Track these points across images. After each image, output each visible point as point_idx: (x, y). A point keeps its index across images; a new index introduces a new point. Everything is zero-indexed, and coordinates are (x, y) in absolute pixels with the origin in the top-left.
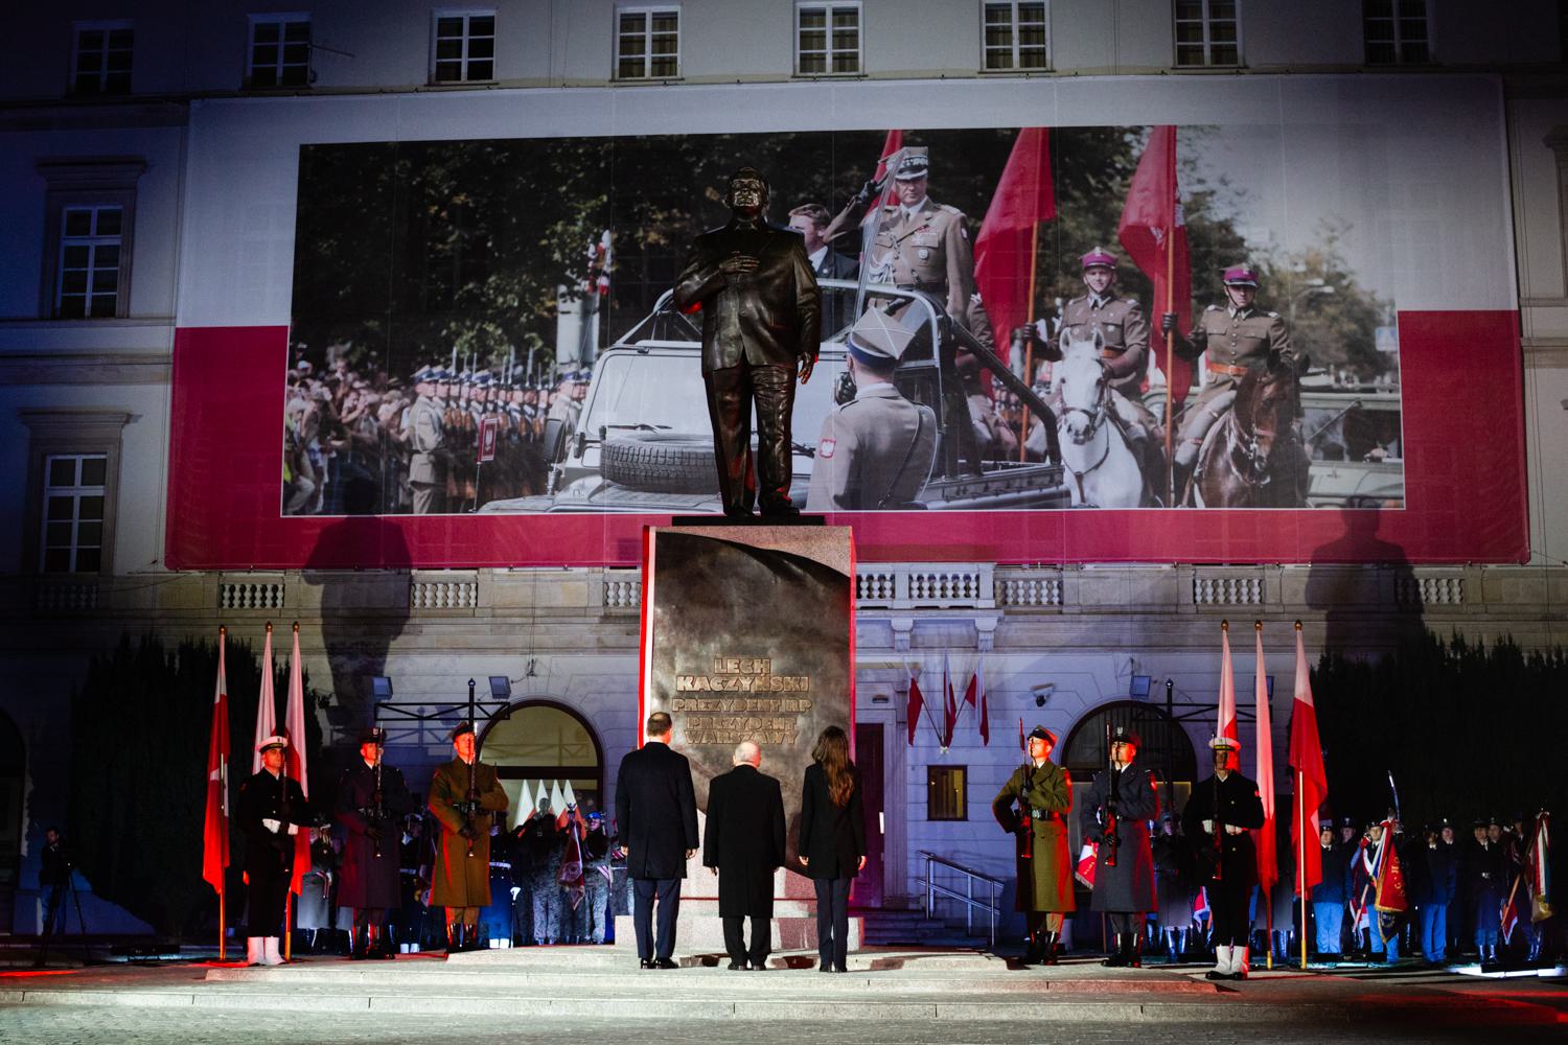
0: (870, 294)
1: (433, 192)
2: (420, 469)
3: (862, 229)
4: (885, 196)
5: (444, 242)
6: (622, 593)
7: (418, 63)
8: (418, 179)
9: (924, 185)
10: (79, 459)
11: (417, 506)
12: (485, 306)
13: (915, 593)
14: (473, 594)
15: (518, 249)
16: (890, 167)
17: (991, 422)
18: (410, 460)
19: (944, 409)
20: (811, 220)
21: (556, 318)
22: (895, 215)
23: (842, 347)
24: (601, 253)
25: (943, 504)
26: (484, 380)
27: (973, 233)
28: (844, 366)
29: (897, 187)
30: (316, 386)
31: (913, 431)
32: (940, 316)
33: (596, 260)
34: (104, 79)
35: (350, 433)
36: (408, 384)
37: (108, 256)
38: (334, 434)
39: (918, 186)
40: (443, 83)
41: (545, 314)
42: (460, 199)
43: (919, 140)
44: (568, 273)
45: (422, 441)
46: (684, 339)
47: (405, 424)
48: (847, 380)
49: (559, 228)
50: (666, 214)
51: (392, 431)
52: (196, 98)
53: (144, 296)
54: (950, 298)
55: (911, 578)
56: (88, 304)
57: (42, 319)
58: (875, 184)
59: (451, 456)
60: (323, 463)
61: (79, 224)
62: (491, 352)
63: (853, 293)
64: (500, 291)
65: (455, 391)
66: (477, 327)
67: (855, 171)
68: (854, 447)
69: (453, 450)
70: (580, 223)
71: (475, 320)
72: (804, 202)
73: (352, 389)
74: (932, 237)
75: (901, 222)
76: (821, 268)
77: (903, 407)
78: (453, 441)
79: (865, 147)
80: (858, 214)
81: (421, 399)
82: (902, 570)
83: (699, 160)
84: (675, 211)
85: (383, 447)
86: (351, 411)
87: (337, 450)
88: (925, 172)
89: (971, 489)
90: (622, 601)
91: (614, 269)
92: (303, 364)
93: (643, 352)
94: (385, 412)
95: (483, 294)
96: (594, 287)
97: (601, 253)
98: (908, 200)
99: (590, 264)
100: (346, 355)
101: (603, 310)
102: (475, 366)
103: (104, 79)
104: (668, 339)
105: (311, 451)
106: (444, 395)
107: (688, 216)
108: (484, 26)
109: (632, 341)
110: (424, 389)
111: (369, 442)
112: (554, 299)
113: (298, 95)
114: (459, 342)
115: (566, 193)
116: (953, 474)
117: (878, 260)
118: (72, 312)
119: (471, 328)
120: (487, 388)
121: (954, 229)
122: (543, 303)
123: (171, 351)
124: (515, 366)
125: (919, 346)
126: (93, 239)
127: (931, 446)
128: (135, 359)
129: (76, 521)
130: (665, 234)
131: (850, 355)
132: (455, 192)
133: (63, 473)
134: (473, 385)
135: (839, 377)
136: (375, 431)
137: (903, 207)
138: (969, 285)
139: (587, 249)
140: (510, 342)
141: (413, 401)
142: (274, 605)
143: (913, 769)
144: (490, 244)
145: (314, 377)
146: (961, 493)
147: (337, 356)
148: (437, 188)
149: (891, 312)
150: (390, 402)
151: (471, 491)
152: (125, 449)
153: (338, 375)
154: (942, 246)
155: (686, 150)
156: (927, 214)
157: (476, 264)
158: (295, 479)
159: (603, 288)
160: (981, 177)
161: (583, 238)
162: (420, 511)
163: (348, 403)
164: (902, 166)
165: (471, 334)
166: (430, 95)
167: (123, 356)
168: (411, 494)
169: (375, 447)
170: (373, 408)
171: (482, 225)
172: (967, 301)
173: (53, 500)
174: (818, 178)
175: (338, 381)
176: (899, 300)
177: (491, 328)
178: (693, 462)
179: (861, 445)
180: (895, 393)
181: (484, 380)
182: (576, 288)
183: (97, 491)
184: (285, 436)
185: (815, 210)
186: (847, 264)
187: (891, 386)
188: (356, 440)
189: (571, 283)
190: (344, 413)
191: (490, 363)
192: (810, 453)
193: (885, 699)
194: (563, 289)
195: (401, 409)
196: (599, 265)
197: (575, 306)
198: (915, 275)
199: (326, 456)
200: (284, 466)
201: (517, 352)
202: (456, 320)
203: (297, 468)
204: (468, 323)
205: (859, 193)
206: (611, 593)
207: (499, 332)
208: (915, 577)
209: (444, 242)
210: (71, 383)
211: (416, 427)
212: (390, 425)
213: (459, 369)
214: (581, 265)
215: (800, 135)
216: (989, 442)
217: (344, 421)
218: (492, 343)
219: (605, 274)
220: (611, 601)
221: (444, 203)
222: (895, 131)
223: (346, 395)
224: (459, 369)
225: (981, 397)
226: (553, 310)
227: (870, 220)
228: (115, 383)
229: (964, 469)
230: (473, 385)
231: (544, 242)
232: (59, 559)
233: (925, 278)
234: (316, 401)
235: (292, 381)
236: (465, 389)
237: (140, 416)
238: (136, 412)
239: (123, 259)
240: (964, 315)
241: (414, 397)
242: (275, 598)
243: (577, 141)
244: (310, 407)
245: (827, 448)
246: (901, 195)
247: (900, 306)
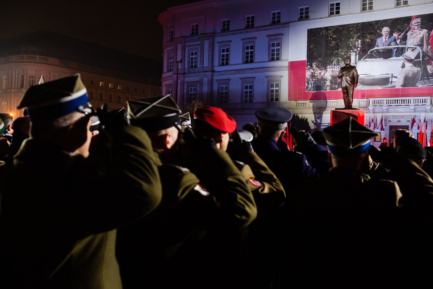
0: (408, 48)
1: (329, 35)
2: (328, 83)
3: (407, 35)
4: (412, 29)
5: (331, 44)
6: (362, 103)
7: (327, 12)
8: (327, 33)
9: (420, 26)
10: (275, 83)
11: (328, 89)
12: (339, 55)
13: (415, 102)
14: (337, 104)
15: (344, 44)
16: (413, 23)
17: (432, 70)
18: (326, 82)
19: (422, 68)
20: (397, 35)
21: (350, 56)
22: (414, 32)
23: (403, 58)
24: (358, 44)
25: (422, 86)
26: (338, 67)
27: (429, 34)
28: (403, 61)
29: (414, 27)
30: (311, 70)
31: (416, 73)
32: (422, 51)
33: (358, 45)
34: (276, 21)
35: (316, 77)
36: (326, 68)
37: (278, 50)
38: (314, 78)
39: (419, 26)
40: (331, 15)
41: (349, 55)
42: (334, 36)
43: (419, 17)
44: (353, 48)
45: (328, 78)
46: (373, 58)
47: (325, 76)
48: (403, 64)
49: (351, 40)
50: (370, 36)
51: (323, 77)
52: (290, 22)
53: (284, 56)
54: (424, 47)
55: (414, 100)
57: (268, 61)
58: (410, 27)
59: (333, 81)
60: (312, 83)
61: (273, 45)
62: (340, 63)
63: (405, 48)
64: (341, 52)
65: (334, 70)
66: (337, 58)
67: (406, 24)
68: (405, 76)
69: (333, 79)
70: (355, 39)
71: (337, 57)
72: (396, 31)
73: (317, 70)
74: (421, 36)
75: (415, 33)
76: (399, 43)
77: (414, 68)
78: (333, 78)
79: (408, 20)
80: (407, 32)
81: (328, 71)
82: (412, 99)
83: (376, 25)
84: (372, 35)
85: (322, 80)
86: (317, 74)
87: (315, 80)
88: (420, 23)
89: (427, 83)
90: (362, 104)
91: (361, 47)
92: (309, 66)
93: (366, 61)
94: (322, 74)
95: (338, 53)
96: (357, 50)
97: (358, 44)
98: (416, 29)
99: (357, 46)
100: (316, 64)
101: (359, 54)
102: (337, 65)
103: (276, 21)
104: (371, 58)
105: (310, 81)
106: (332, 70)
107: (374, 36)
108: (338, 4)
109: (364, 59)
110: (328, 70)
111: (320, 79)
112: (350, 53)
113: (307, 20)
114: (334, 61)
115: (352, 34)
116: (424, 80)
117: (410, 41)
118: (273, 60)
119: (336, 59)
120: (339, 69)
121: (425, 34)
122: (348, 54)
123: (288, 65)
124: (344, 65)
125: (418, 57)
127: (419, 75)
128: (282, 67)
129: (275, 93)
130: (370, 39)
131: (404, 59)
132: (333, 35)
133: (272, 86)
134: (337, 68)
135: (402, 63)
136: (321, 77)
137: (415, 31)
138: (428, 44)
139: (356, 43)
140: (343, 61)
141: (327, 72)
142: (305, 106)
143: (414, 133)
144: (339, 44)
145: (310, 68)
146: (425, 83)
147: (314, 65)
148: (330, 35)
149: (412, 51)
150: (323, 72)
151: (336, 86)
152: (281, 82)
153: (314, 68)
154: (423, 37)
155: (374, 24)
156: (420, 31)
157: (337, 47)
158: (308, 85)
159: (359, 50)
160: (431, 23)
161: (355, 41)
162: (328, 90)
163: (316, 73)
164: (415, 23)
165: (336, 60)
166: (329, 18)
168: (327, 87)
169: (321, 80)
170: (320, 73)
171: (338, 40)
172: (427, 47)
173: (271, 90)
174: (399, 26)
175: (314, 69)
176: (414, 48)
177: (339, 58)
178: (375, 80)
179: (406, 75)
180: (413, 66)
181: (338, 67)
182: (354, 50)
183: (277, 88)
184: (306, 78)
185: (398, 33)
186: (404, 42)
187: (412, 64)
188: (317, 79)
189: (353, 50)
190: (315, 74)
191: (339, 64)
192: (396, 77)
193: (409, 121)
194: (352, 51)
195: (325, 73)
196: (358, 46)
197: (354, 54)
198: (417, 43)
199: (313, 82)
200: (306, 83)
201: (344, 62)
202: (334, 57)
203: (308, 83)
204: (336, 58)
205: (407, 28)
206: (360, 103)
207: (341, 59)
208: (415, 99)
209: (331, 44)
211: (327, 76)
212: (323, 76)
213: (334, 66)
214: (355, 46)
215: (395, 18)
216: (431, 74)
217: (316, 75)
218: (340, 61)
219: (359, 48)
220: (360, 104)
221: (331, 37)
222: (414, 16)
223: (316, 71)
224: (334, 66)
225: (430, 66)
226: (350, 55)
227: (409, 34)
229: (426, 79)
230: (337, 68)
231: (349, 43)
232: (272, 99)
233: (419, 44)
234: (311, 73)
235: (307, 69)
236: (335, 69)
238: (283, 75)
239: (280, 51)
240: (427, 50)
241: (327, 71)
242: (305, 105)
243: (354, 24)
244: (310, 73)
245: (399, 76)
246: (415, 28)
247: (414, 49)
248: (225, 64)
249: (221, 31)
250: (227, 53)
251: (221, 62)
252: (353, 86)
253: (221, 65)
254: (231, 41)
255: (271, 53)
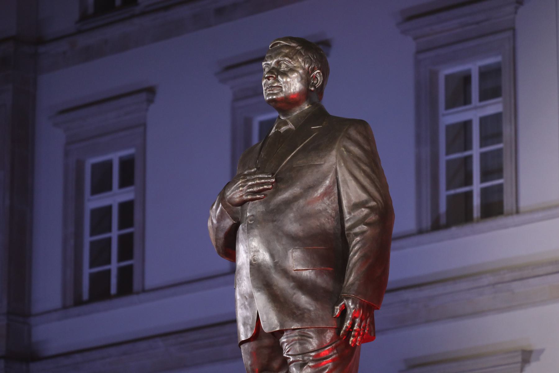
56: (476, 201)
57: (421, 232)
126: (476, 108)
167: (512, 269)
210: (456, 317)
228: (509, 308)
237: (541, 351)
238: (536, 346)
239: (507, 130)
248: (113, 290)
249: (84, 17)
250: (127, 194)
251: (87, 271)
252: (334, 324)
253: (86, 296)
254: (151, 91)
255: (443, 158)
